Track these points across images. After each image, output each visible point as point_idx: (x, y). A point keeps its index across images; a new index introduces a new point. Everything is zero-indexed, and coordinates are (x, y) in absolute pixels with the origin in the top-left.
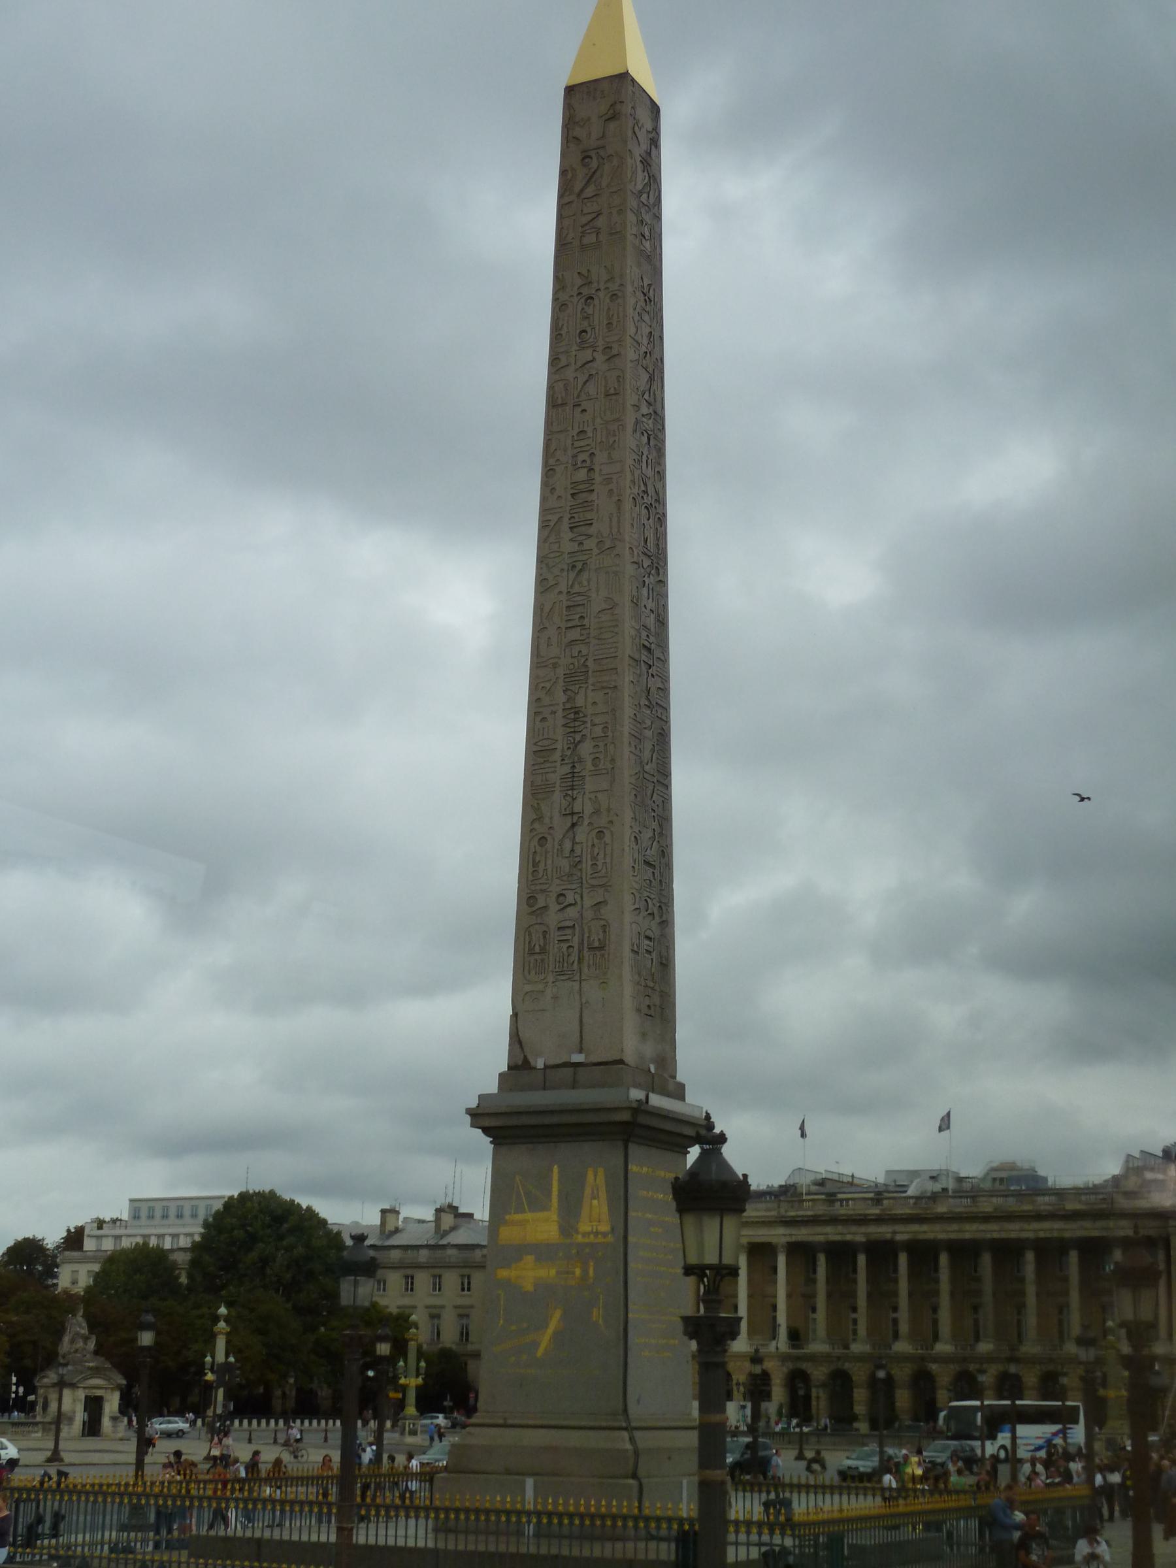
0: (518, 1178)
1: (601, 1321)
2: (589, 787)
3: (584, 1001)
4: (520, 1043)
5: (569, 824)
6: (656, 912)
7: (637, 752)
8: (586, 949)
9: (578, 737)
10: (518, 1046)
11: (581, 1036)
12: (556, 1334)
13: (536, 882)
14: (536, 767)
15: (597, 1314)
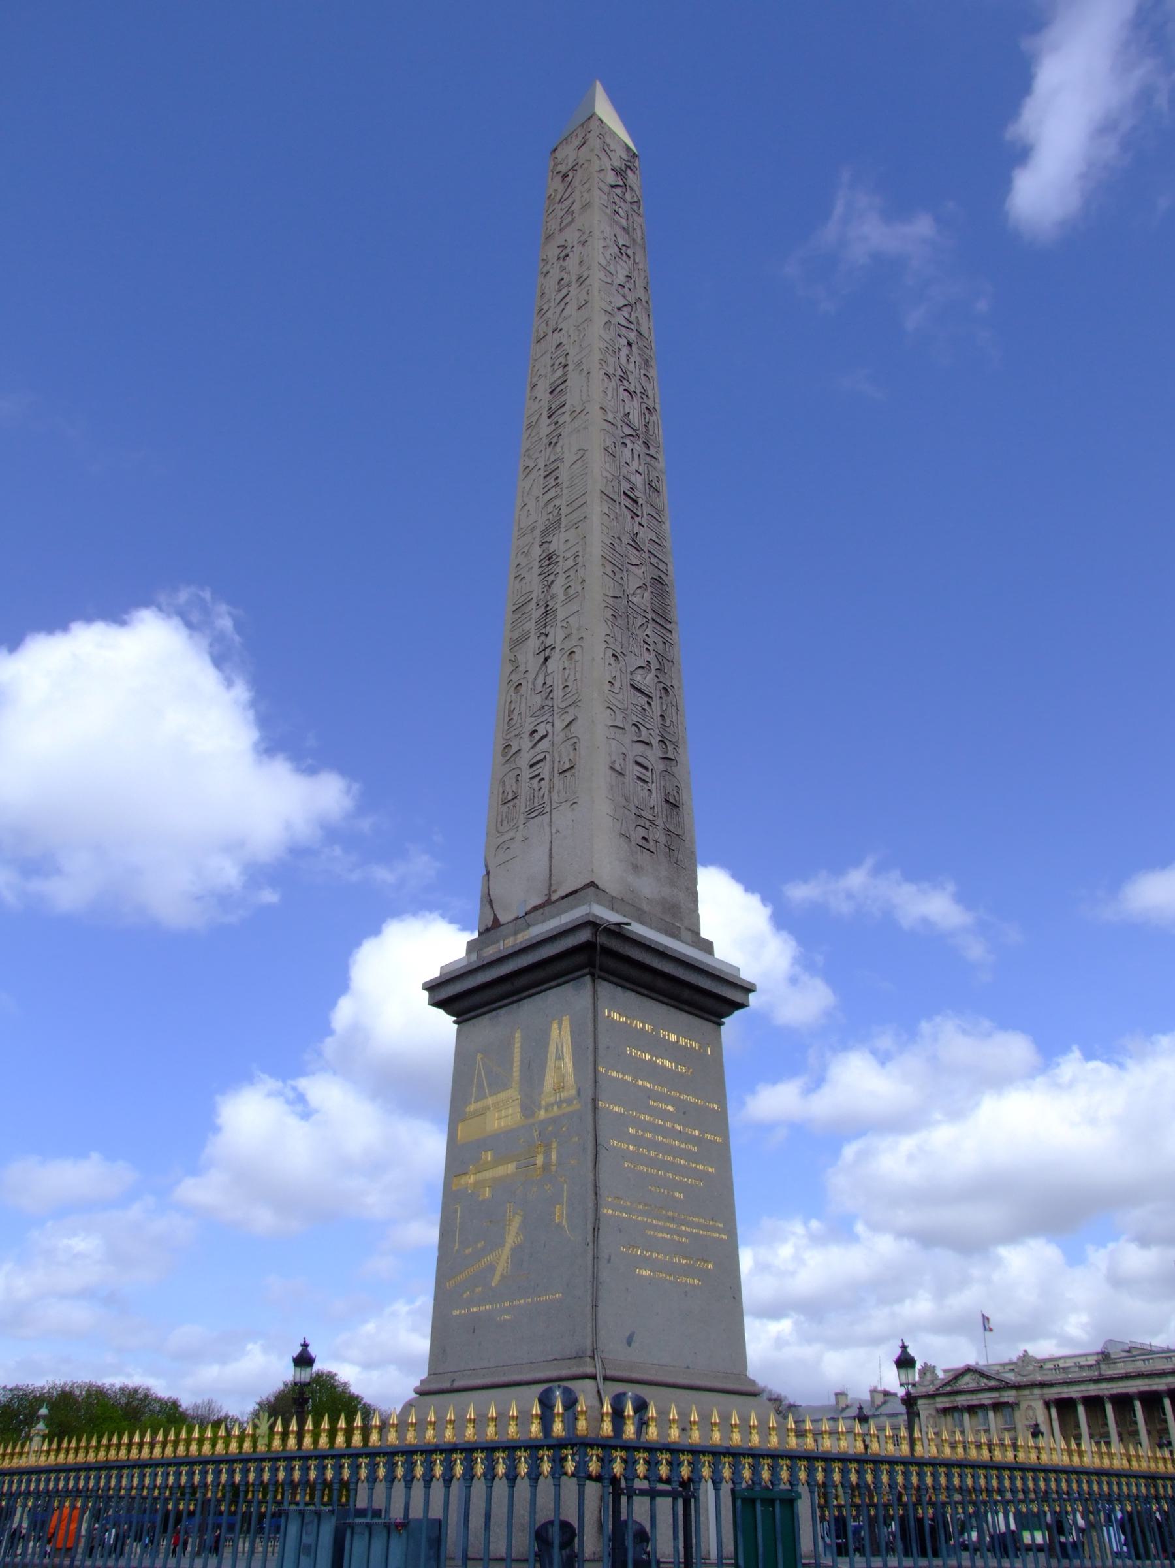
0: (479, 1057)
1: (564, 1223)
2: (561, 615)
3: (554, 831)
4: (491, 902)
5: (542, 660)
6: (655, 742)
7: (620, 581)
8: (556, 775)
9: (551, 578)
10: (489, 907)
11: (550, 870)
12: (517, 1250)
13: (512, 729)
14: (514, 624)
15: (560, 1214)
